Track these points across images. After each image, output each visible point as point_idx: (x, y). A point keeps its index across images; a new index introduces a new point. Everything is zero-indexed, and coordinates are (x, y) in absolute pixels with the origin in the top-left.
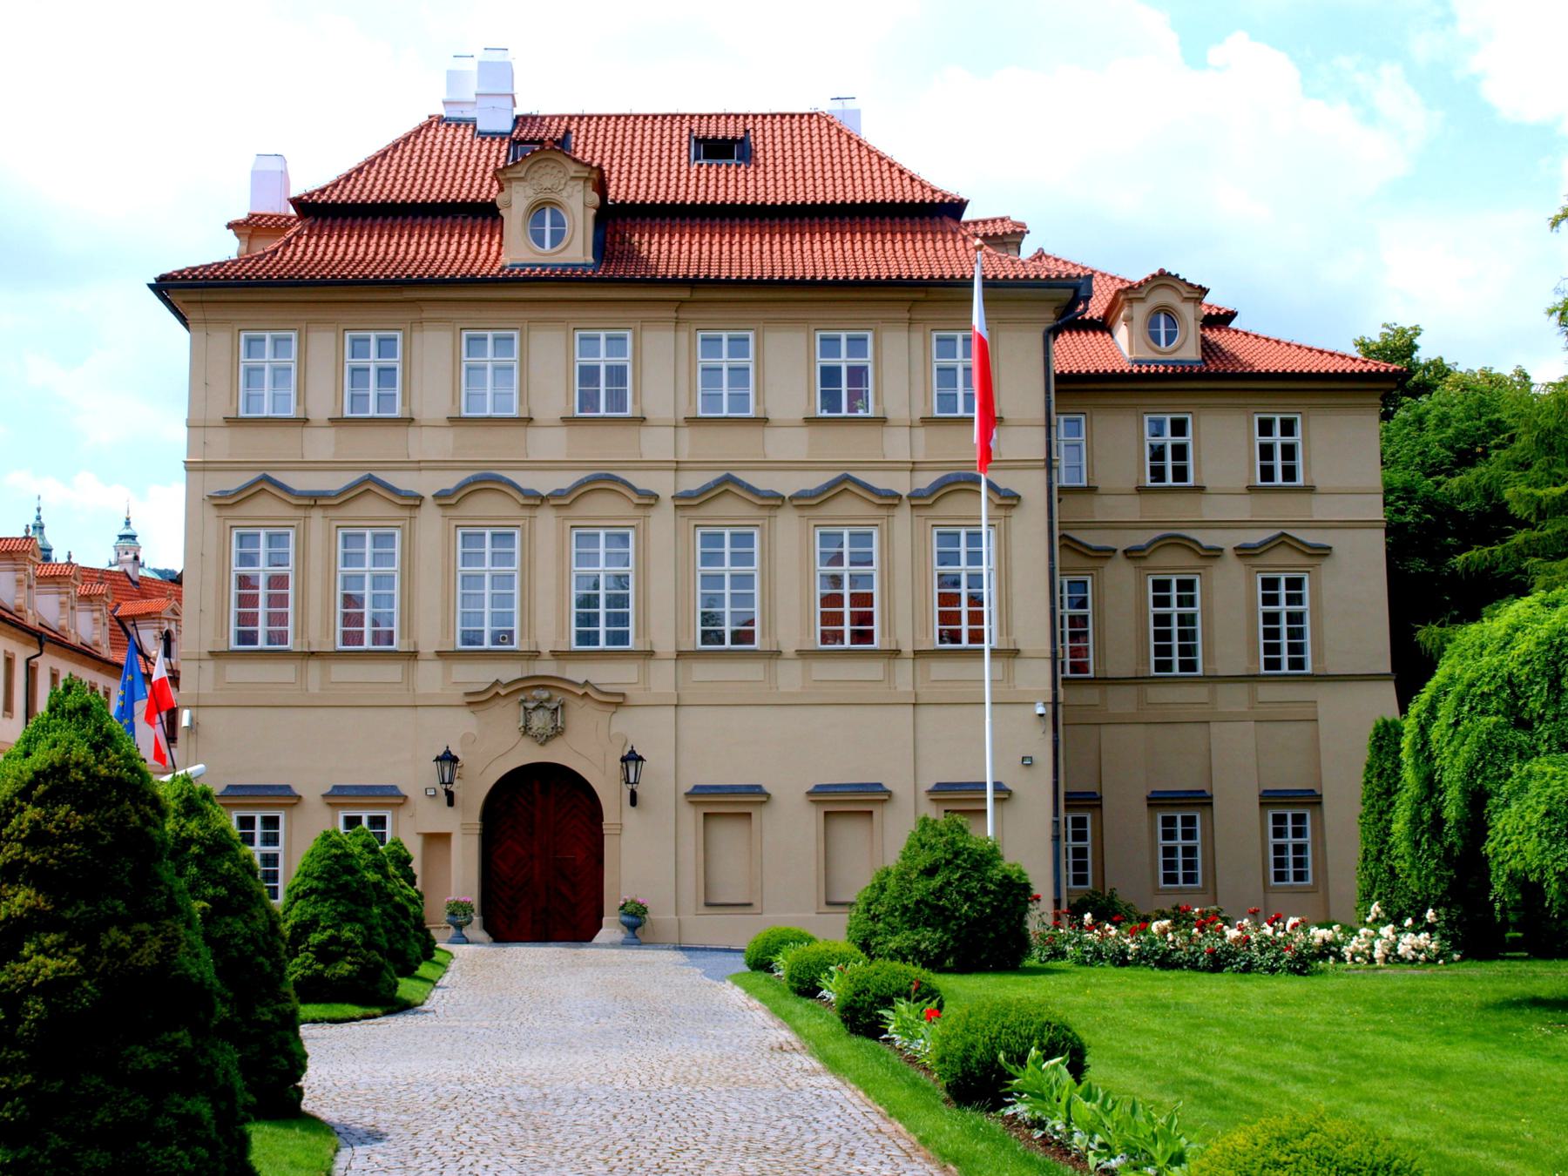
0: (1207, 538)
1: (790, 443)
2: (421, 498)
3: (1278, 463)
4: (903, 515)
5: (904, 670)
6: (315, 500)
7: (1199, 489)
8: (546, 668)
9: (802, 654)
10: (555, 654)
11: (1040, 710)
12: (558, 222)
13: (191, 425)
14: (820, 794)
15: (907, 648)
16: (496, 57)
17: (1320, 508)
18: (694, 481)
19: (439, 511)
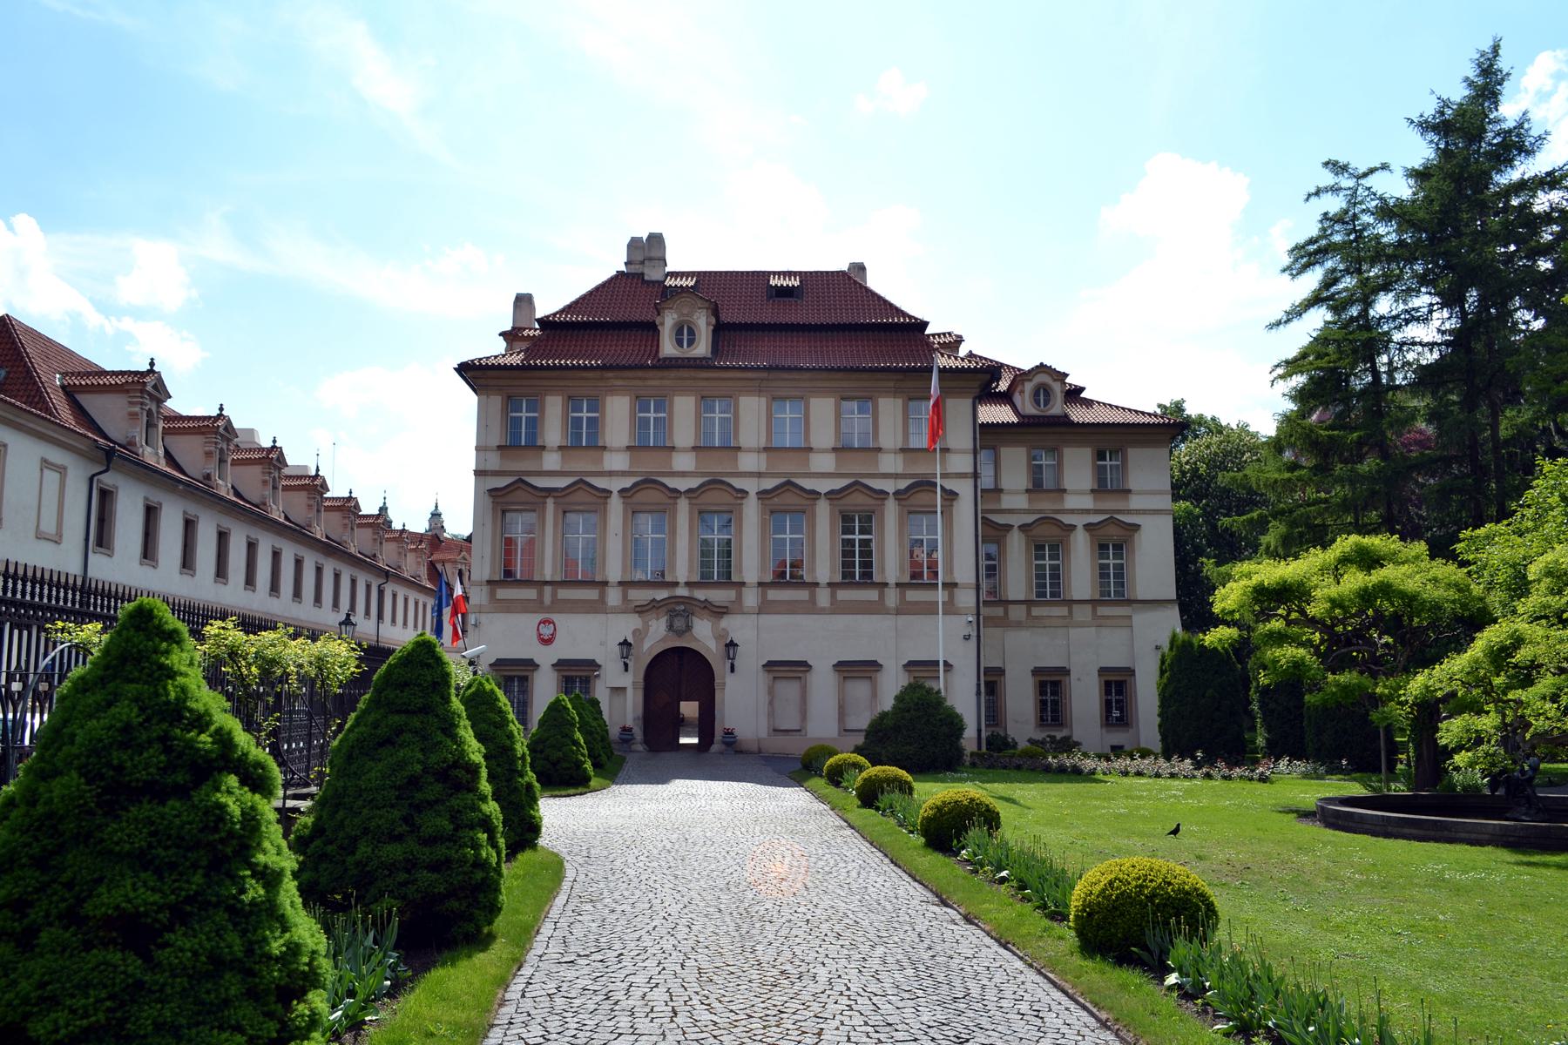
8: (682, 592)
10: (688, 584)
11: (970, 619)
12: (691, 332)
13: (477, 449)
14: (841, 666)
18: (769, 484)
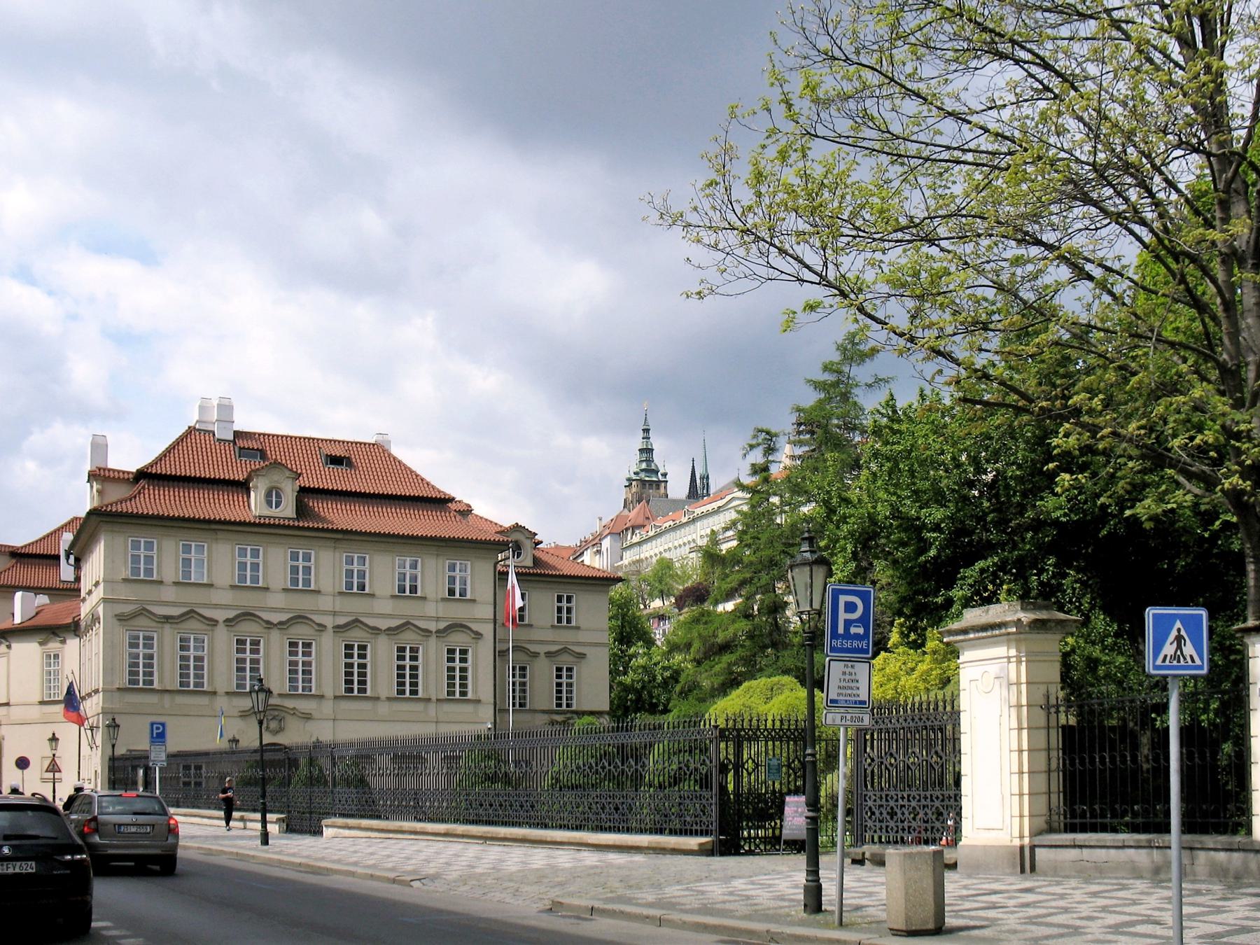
0: (533, 648)
1: (384, 606)
2: (217, 621)
3: (564, 615)
4: (433, 641)
5: (432, 708)
6: (167, 619)
7: (530, 626)
9: (389, 699)
10: (280, 695)
15: (434, 698)
16: (226, 402)
17: (582, 637)
18: (342, 621)
19: (226, 628)
